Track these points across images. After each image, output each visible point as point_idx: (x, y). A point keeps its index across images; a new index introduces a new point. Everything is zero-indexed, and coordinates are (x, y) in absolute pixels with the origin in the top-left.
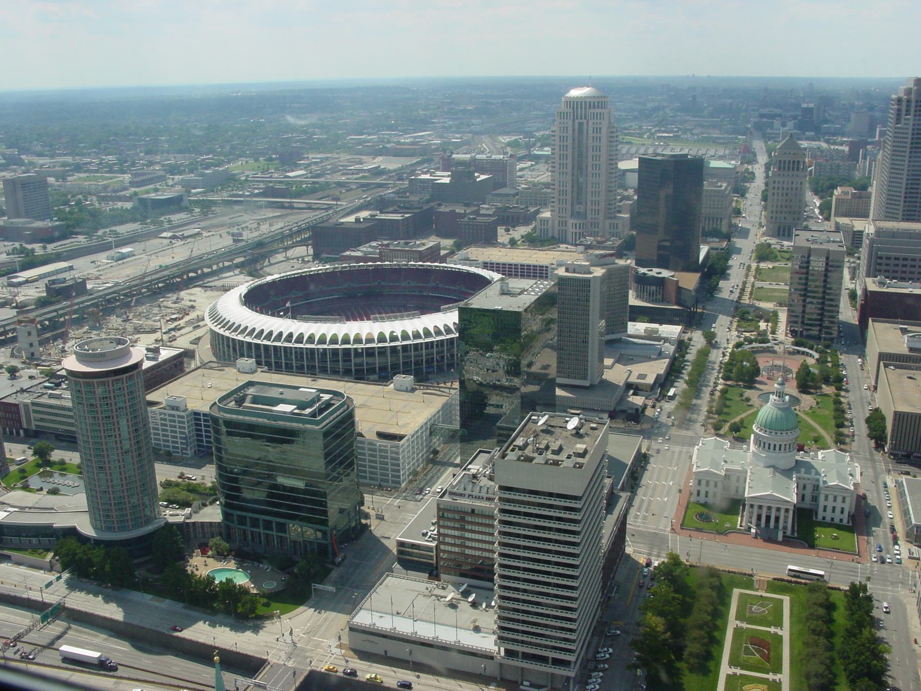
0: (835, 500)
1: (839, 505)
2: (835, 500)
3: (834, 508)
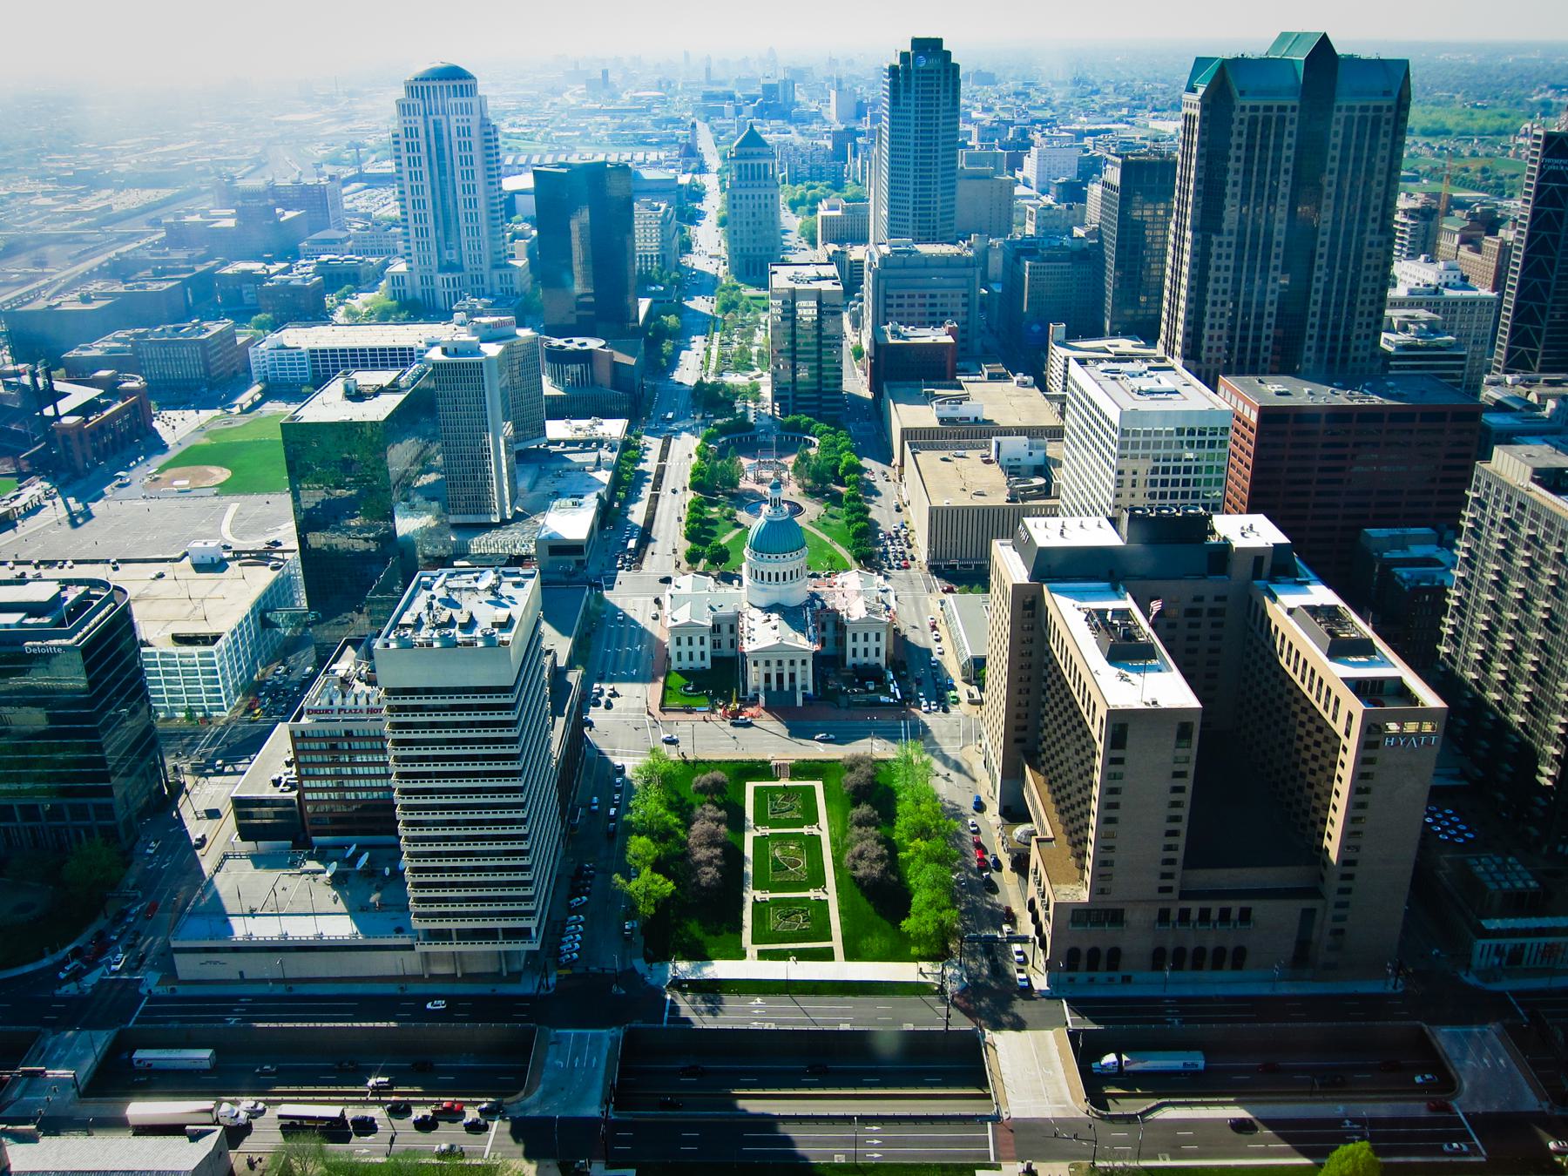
0: (690, 643)
1: (697, 648)
2: (690, 643)
3: (691, 654)
